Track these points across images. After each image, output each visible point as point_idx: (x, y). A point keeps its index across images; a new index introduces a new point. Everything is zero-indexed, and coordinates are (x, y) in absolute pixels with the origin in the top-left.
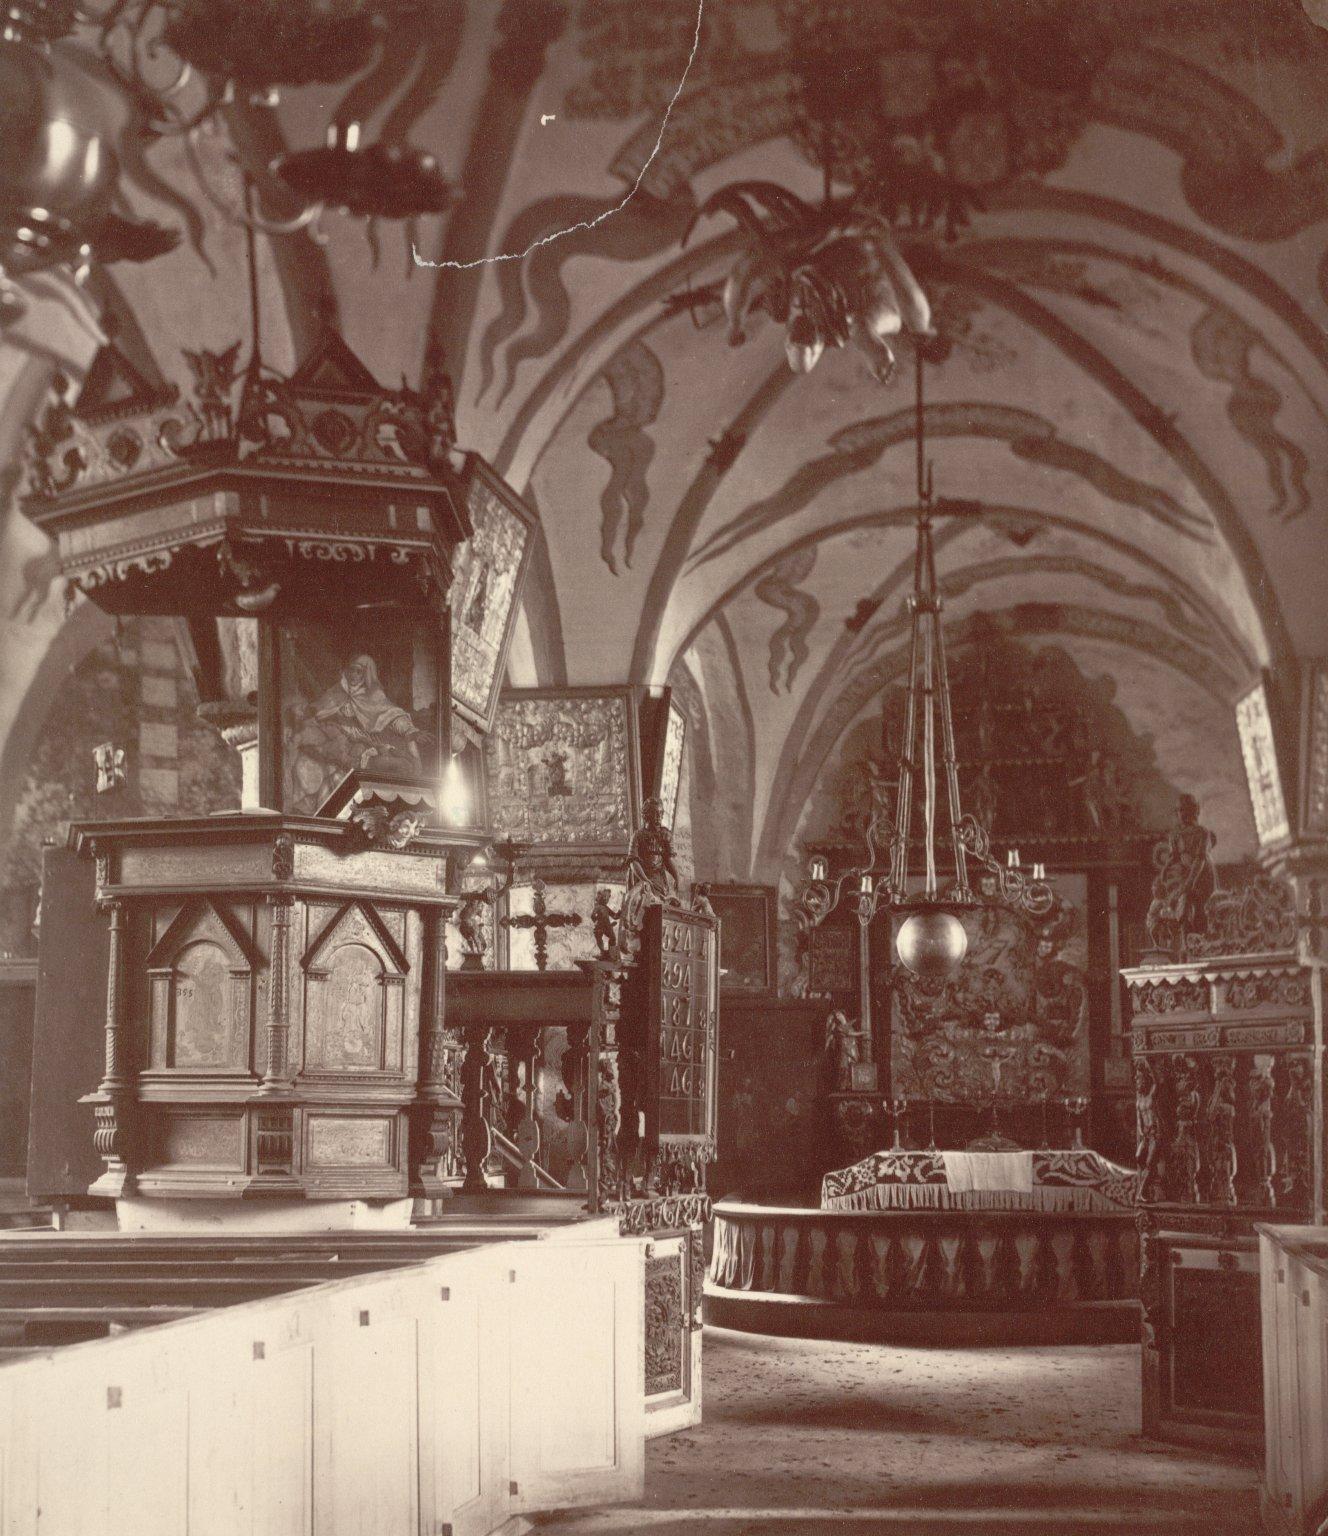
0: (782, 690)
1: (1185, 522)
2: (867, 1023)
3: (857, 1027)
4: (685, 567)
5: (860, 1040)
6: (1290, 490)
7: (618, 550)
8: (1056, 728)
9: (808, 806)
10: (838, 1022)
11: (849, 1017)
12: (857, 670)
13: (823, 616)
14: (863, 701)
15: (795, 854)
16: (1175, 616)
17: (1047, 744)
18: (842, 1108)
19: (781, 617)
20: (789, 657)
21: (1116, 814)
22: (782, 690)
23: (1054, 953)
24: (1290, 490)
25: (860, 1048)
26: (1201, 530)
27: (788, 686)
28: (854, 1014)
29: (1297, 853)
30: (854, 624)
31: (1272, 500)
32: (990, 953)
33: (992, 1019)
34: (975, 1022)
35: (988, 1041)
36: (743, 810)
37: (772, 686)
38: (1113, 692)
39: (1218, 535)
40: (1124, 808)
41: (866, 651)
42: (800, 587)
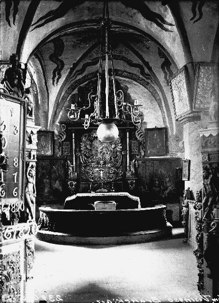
0: (56, 85)
1: (165, 25)
2: (74, 163)
3: (72, 164)
4: (31, 28)
5: (73, 168)
6: (198, 12)
7: (11, 20)
9: (61, 113)
12: (72, 82)
13: (66, 67)
14: (73, 89)
15: (59, 124)
16: (143, 73)
19: (55, 66)
20: (57, 77)
22: (56, 85)
24: (198, 12)
26: (169, 27)
27: (57, 83)
29: (192, 115)
30: (72, 70)
31: (191, 15)
33: (101, 162)
36: (46, 114)
37: (53, 84)
39: (175, 28)
41: (74, 77)
42: (60, 58)
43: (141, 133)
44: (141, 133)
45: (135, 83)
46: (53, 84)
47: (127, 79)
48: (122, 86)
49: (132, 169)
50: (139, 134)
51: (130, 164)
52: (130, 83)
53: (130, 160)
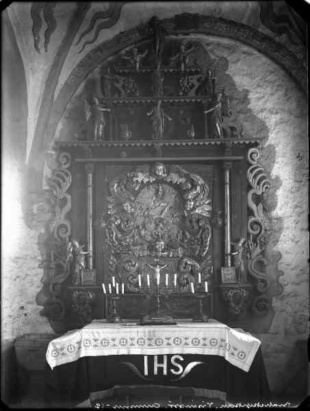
0: (42, 51)
3: (85, 249)
5: (87, 257)
8: (197, 85)
10: (74, 246)
11: (80, 244)
17: (192, 93)
18: (75, 294)
21: (229, 131)
22: (42, 51)
23: (194, 208)
25: (87, 261)
27: (46, 47)
28: (84, 243)
32: (159, 209)
34: (152, 248)
35: (156, 257)
38: (225, 63)
40: (232, 129)
41: (93, 33)
43: (260, 172)
44: (260, 172)
45: (245, 48)
46: (36, 46)
47: (226, 41)
48: (213, 57)
49: (240, 262)
50: (255, 177)
51: (233, 249)
52: (231, 49)
53: (235, 240)
